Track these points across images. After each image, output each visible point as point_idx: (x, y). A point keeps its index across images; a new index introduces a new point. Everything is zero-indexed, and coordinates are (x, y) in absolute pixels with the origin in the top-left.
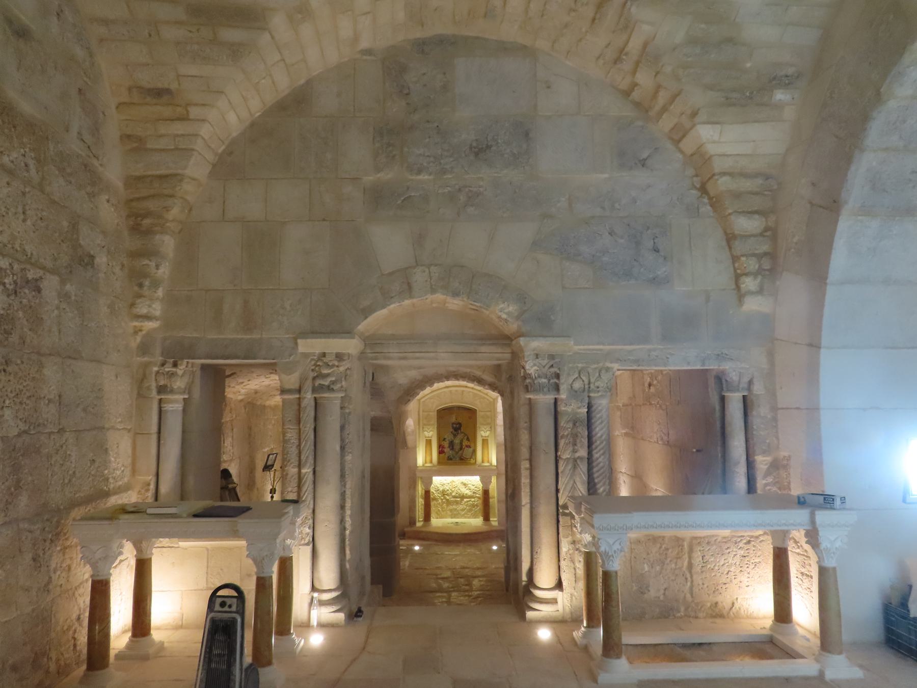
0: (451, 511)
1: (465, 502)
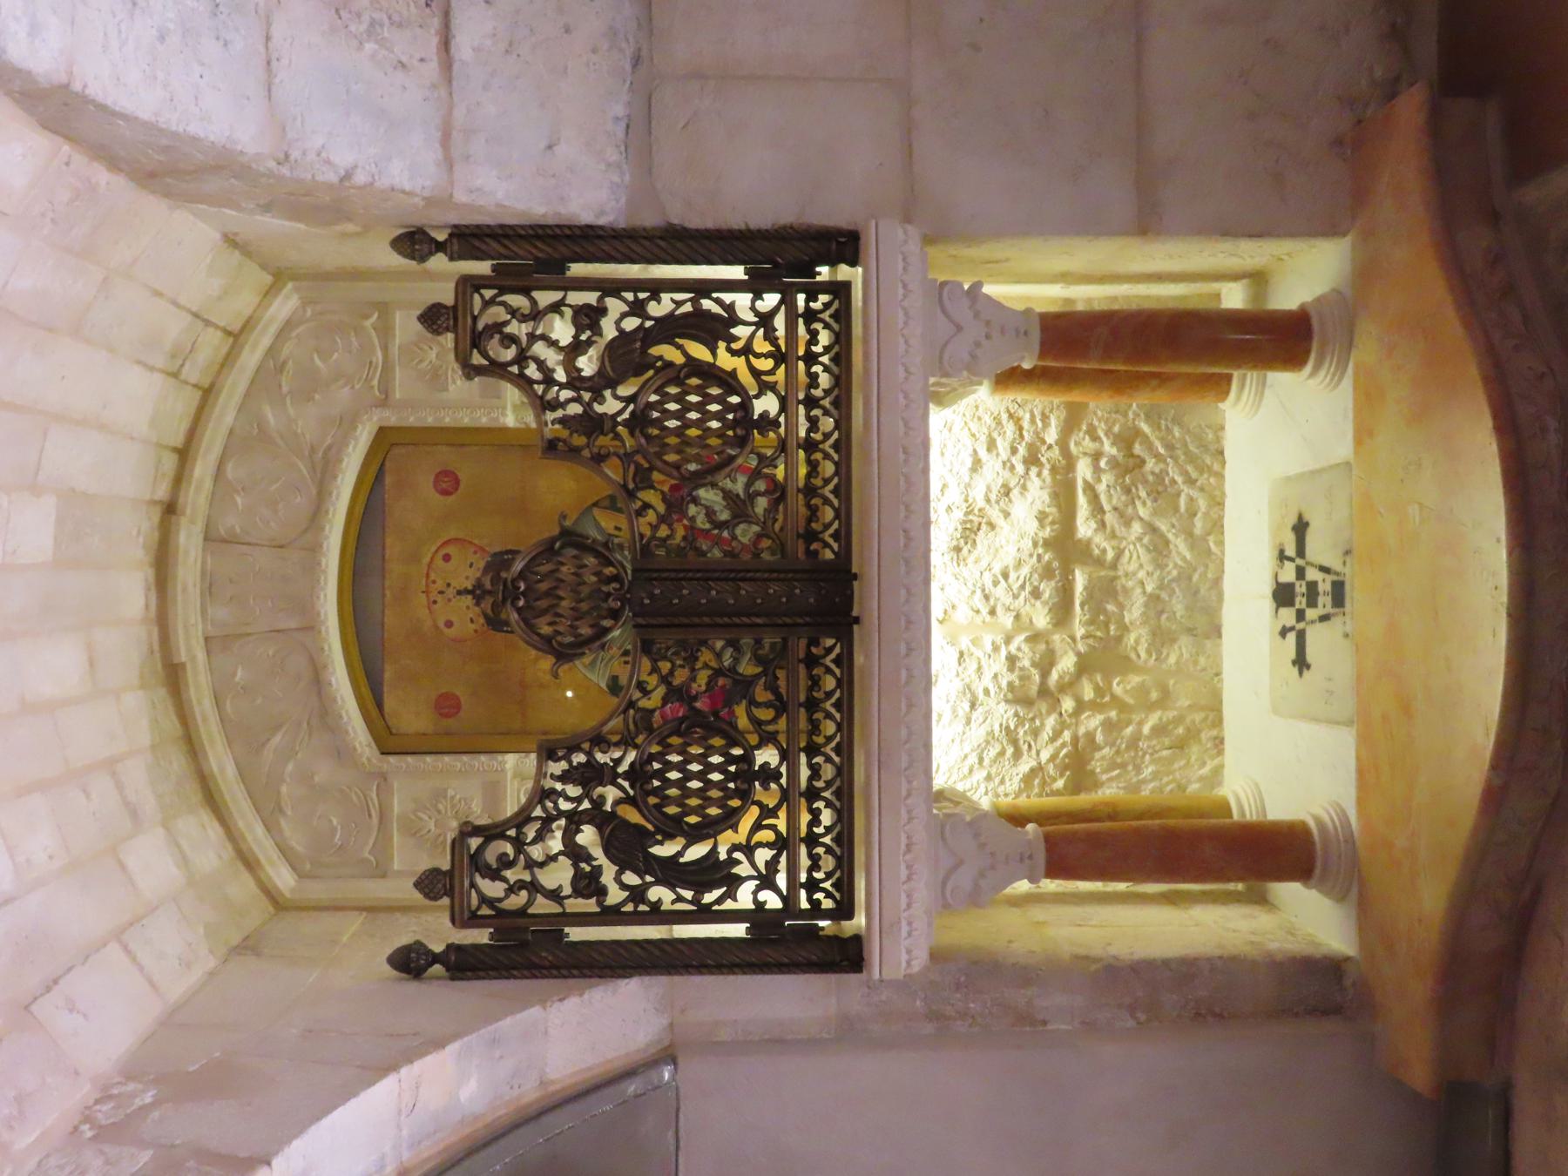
0: (1161, 639)
1: (1102, 525)
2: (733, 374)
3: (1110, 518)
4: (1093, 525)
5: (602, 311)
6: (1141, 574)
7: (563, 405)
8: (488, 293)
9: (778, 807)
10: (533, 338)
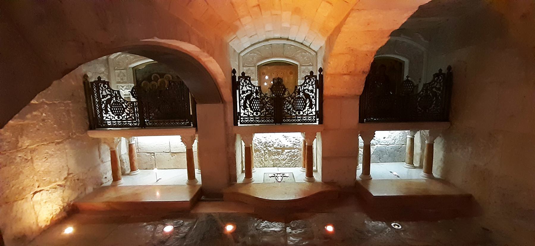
0: (273, 160)
2: (305, 109)
3: (287, 154)
4: (287, 152)
5: (313, 93)
6: (280, 158)
7: (301, 88)
8: (315, 79)
9: (253, 115)
10: (309, 85)
